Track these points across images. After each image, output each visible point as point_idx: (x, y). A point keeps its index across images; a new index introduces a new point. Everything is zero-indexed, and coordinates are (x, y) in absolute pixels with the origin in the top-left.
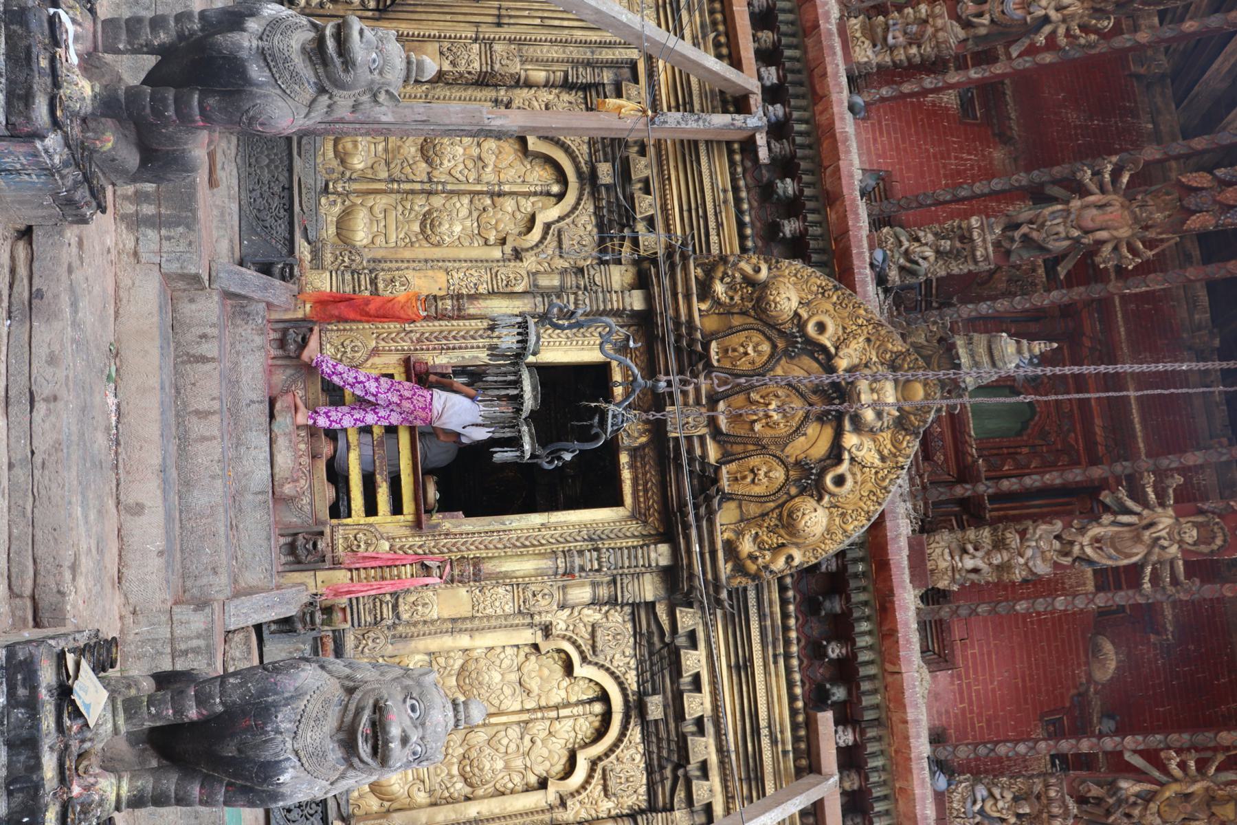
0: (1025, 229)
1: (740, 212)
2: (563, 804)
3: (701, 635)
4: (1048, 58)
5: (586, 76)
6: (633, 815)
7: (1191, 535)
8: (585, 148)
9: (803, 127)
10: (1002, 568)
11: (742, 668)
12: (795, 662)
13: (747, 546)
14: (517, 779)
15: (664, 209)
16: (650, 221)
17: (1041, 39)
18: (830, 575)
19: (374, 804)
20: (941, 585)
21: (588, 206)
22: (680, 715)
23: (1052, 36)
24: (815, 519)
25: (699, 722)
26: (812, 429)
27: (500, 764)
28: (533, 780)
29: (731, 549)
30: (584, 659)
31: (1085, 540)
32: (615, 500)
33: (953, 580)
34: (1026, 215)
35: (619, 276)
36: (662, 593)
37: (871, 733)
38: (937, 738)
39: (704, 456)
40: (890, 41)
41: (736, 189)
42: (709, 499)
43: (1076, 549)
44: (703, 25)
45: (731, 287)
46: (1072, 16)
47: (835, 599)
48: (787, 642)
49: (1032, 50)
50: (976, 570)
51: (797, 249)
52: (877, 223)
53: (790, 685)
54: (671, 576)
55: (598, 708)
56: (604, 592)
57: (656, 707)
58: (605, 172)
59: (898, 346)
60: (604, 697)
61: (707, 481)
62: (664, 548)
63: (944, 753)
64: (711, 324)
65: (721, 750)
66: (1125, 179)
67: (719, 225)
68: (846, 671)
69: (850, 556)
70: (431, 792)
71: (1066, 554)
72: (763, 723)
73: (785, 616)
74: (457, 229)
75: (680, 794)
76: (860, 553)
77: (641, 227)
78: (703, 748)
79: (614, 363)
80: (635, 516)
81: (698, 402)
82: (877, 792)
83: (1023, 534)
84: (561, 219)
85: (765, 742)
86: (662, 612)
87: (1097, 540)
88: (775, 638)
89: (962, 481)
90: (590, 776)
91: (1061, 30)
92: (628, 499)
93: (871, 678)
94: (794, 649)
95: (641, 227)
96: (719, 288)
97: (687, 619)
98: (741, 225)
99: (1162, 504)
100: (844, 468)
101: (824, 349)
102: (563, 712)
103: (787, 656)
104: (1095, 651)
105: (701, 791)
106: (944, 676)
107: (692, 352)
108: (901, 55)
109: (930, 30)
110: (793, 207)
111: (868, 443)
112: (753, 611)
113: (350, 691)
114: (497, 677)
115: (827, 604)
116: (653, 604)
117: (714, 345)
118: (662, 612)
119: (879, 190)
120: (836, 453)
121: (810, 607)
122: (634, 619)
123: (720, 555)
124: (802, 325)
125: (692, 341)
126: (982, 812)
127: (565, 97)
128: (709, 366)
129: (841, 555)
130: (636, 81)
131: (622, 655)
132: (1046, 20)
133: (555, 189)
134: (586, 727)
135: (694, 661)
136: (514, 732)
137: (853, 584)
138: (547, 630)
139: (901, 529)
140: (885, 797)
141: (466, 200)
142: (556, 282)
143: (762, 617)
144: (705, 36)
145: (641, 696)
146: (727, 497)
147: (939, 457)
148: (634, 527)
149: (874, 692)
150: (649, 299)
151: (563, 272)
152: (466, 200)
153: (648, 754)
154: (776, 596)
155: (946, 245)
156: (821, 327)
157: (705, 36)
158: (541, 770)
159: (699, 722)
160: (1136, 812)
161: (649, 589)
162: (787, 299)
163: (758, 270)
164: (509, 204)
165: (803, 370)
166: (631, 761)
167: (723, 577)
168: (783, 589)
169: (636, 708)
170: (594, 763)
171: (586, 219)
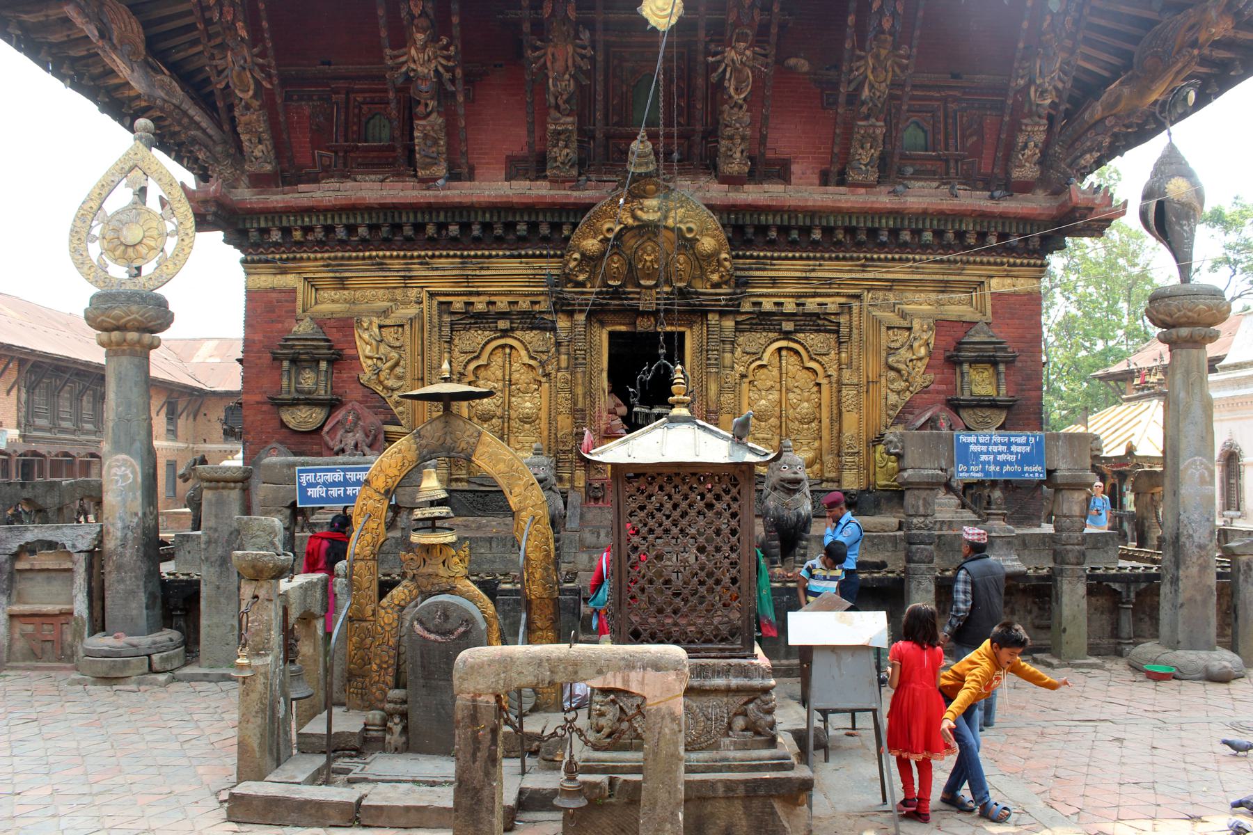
0: (560, 102)
1: (534, 256)
2: (829, 376)
3: (755, 299)
4: (459, 72)
5: (446, 330)
7: (742, 45)
8: (487, 333)
9: (487, 216)
10: (743, 138)
11: (774, 282)
12: (776, 255)
13: (715, 277)
14: (813, 396)
16: (533, 303)
17: (447, 76)
18: (733, 232)
19: (816, 467)
20: (747, 170)
21: (518, 334)
23: (447, 69)
24: (707, 244)
25: (798, 305)
26: (660, 240)
27: (806, 404)
28: (815, 389)
29: (715, 286)
30: (759, 359)
31: (736, 97)
33: (746, 164)
34: (552, 100)
35: (562, 323)
36: (731, 317)
37: (817, 222)
39: (667, 293)
40: (435, 155)
41: (520, 256)
42: (689, 293)
43: (740, 102)
44: (421, 264)
45: (580, 271)
46: (434, 53)
47: (745, 229)
48: (765, 257)
49: (453, 81)
50: (742, 152)
51: (556, 227)
53: (786, 258)
54: (722, 314)
55: (784, 353)
56: (728, 347)
57: (788, 326)
58: (502, 324)
60: (780, 350)
61: (682, 293)
62: (710, 316)
63: (834, 178)
64: (598, 281)
65: (815, 295)
66: (539, 43)
67: (540, 268)
68: (784, 230)
69: (726, 221)
70: (815, 439)
71: (741, 107)
72: (804, 275)
73: (751, 257)
74: (528, 404)
76: (725, 216)
77: (537, 308)
78: (811, 305)
79: (610, 329)
81: (638, 293)
82: (847, 223)
83: (727, 126)
84: (527, 349)
85: (813, 275)
86: (740, 318)
87: (736, 89)
88: (762, 263)
89: (695, 152)
90: (818, 361)
91: (444, 62)
92: (681, 329)
93: (789, 218)
94: (769, 254)
95: (537, 308)
96: (581, 277)
97: (746, 307)
98: (541, 256)
99: (723, 52)
100: (683, 227)
101: (621, 230)
102: (784, 370)
103: (772, 258)
104: (792, 70)
105: (832, 308)
106: (795, 168)
107: (613, 293)
108: (444, 149)
109: (431, 133)
110: (533, 227)
111: (672, 214)
112: (747, 274)
113: (776, 489)
114: (763, 402)
115: (750, 236)
116: (737, 323)
117: (610, 282)
118: (740, 318)
121: (749, 244)
122: (743, 331)
123: (718, 291)
124: (606, 240)
125: (607, 293)
126: (866, 165)
127: (456, 342)
128: (620, 286)
129: (724, 226)
131: (760, 337)
132: (436, 71)
133: (508, 351)
134: (793, 359)
135: (768, 305)
136: (791, 396)
137: (740, 222)
138: (743, 376)
139: (718, 192)
140: (850, 218)
141: (513, 399)
142: (564, 357)
143: (751, 269)
144: (427, 264)
145: (780, 331)
146: (689, 285)
148: (696, 328)
149: (797, 217)
151: (558, 351)
152: (513, 399)
153: (811, 331)
154: (741, 261)
155: (561, 144)
156: (610, 230)
157: (427, 264)
158: (811, 384)
159: (798, 305)
160: (878, 94)
161: (729, 323)
162: (591, 244)
163: (575, 259)
164: (515, 376)
165: (631, 242)
166: (815, 340)
167: (729, 291)
168: (737, 257)
169: (787, 335)
170: (811, 359)
171: (529, 336)
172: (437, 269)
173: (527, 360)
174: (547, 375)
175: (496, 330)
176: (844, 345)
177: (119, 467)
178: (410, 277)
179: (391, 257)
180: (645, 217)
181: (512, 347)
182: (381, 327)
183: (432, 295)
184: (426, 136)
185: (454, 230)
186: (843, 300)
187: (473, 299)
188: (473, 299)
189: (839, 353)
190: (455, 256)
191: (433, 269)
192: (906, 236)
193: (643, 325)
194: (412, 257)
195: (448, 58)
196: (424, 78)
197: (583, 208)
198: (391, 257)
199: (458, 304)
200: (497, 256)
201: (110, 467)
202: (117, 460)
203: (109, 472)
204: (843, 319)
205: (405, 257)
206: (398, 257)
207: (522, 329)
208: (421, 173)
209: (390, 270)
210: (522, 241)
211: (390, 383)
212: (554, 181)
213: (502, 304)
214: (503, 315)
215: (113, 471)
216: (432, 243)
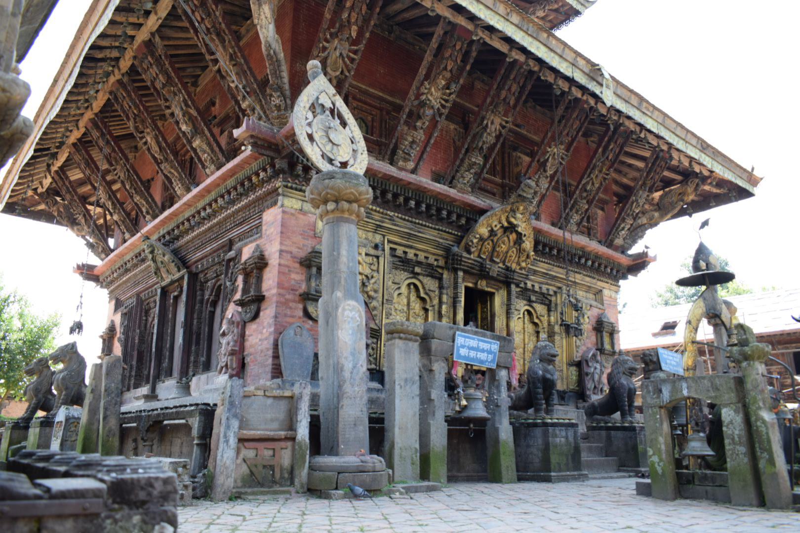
1: (445, 231)
6: (549, 310)
13: (523, 264)
15: (434, 254)
16: (436, 260)
21: (421, 277)
22: (536, 292)
32: (492, 295)
38: (553, 224)
41: (438, 230)
52: (451, 184)
58: (417, 270)
59: (508, 208)
75: (549, 297)
77: (435, 263)
80: (497, 290)
91: (443, 102)
105: (551, 293)
119: (437, 178)
120: (519, 235)
130: (395, 250)
133: (412, 287)
147: (495, 190)
148: (501, 291)
150: (461, 269)
170: (537, 317)
172: (397, 226)
173: (422, 295)
174: (433, 306)
175: (413, 272)
176: (552, 313)
177: (351, 311)
178: (381, 227)
179: (375, 211)
180: (515, 222)
181: (415, 286)
182: (367, 255)
183: (389, 242)
184: (413, 142)
185: (412, 203)
186: (555, 289)
187: (407, 250)
188: (407, 250)
189: (549, 316)
190: (408, 221)
191: (395, 225)
192: (583, 261)
193: (483, 285)
194: (386, 214)
195: (446, 101)
196: (432, 107)
197: (482, 212)
198: (375, 211)
199: (400, 251)
200: (428, 227)
201: (344, 310)
202: (349, 305)
203: (343, 314)
204: (553, 299)
205: (382, 213)
206: (379, 212)
207: (424, 275)
208: (401, 163)
209: (372, 219)
210: (440, 220)
211: (372, 293)
212: (461, 191)
213: (421, 257)
214: (419, 263)
215: (346, 313)
216: (397, 208)
